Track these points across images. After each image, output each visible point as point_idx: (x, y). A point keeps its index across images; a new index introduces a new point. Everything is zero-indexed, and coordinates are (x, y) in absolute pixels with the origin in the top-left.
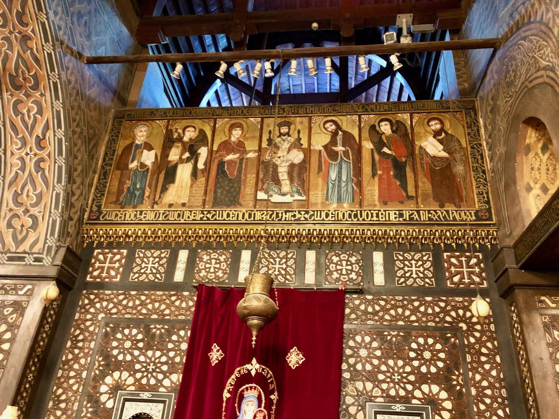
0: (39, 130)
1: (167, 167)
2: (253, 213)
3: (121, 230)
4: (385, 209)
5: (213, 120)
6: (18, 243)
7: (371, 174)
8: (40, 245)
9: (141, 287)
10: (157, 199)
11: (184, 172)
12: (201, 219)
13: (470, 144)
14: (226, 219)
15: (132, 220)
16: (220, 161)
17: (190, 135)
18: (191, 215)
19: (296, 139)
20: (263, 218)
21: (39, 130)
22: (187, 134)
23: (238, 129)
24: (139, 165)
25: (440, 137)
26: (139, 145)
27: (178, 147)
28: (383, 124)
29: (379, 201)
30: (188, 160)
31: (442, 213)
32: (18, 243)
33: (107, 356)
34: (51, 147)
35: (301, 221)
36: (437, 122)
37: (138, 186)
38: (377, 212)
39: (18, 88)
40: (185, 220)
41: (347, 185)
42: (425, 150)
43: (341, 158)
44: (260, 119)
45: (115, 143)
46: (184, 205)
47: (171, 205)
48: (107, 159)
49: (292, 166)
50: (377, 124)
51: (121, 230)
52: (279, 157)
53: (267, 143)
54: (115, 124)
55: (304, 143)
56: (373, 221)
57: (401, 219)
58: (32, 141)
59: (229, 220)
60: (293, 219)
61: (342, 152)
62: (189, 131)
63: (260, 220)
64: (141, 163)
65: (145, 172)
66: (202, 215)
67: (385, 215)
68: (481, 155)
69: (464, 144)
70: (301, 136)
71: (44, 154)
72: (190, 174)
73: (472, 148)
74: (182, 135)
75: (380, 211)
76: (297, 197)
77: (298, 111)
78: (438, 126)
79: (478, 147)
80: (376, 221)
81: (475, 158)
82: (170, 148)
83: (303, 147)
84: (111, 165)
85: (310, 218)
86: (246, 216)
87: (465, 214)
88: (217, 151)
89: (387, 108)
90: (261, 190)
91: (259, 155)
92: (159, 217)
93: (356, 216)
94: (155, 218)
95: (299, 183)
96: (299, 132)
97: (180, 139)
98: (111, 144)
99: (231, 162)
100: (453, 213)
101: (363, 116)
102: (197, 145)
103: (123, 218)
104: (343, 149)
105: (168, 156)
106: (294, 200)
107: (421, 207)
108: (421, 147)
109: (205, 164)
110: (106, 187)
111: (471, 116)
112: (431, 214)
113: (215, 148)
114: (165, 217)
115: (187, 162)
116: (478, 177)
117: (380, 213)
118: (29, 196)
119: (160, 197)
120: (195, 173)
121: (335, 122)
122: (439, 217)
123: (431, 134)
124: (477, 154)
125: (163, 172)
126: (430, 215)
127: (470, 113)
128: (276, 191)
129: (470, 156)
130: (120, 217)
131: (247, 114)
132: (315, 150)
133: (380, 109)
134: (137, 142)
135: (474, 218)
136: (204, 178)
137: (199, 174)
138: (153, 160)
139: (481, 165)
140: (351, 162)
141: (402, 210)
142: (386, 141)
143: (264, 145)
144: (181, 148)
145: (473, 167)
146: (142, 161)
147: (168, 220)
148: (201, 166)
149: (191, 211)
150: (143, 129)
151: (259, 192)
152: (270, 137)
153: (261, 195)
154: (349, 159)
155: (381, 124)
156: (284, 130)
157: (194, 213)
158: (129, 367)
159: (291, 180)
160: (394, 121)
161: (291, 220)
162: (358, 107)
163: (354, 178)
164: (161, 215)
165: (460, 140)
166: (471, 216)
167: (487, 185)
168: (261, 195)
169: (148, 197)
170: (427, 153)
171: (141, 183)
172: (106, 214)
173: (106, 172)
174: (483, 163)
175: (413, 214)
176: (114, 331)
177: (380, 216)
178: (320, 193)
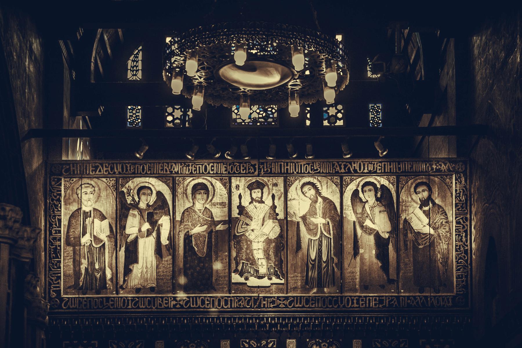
1: (127, 242)
2: (229, 298)
4: (366, 295)
5: (171, 179)
7: (353, 253)
10: (121, 283)
12: (175, 306)
13: (456, 218)
14: (201, 306)
15: (98, 308)
16: (185, 235)
18: (162, 301)
19: (271, 207)
20: (240, 305)
22: (143, 198)
23: (202, 191)
24: (92, 239)
25: (426, 208)
26: (88, 213)
27: (134, 216)
28: (367, 188)
29: (360, 286)
30: (149, 233)
31: (421, 299)
35: (280, 308)
36: (425, 188)
37: (97, 267)
38: (357, 298)
40: (156, 308)
41: (327, 265)
42: (409, 224)
43: (322, 233)
44: (227, 178)
45: (58, 211)
46: (152, 289)
47: (138, 290)
48: (53, 232)
49: (268, 241)
50: (360, 189)
52: (253, 230)
53: (238, 211)
54: (53, 183)
55: (280, 210)
56: (354, 307)
57: (381, 306)
59: (205, 308)
60: (272, 306)
61: (322, 225)
62: (144, 194)
63: (237, 308)
64: (94, 236)
65: (102, 249)
66: (174, 302)
67: (366, 302)
68: (466, 232)
69: (450, 219)
70: (276, 204)
72: (153, 251)
73: (457, 223)
74: (137, 199)
75: (361, 297)
76: (275, 280)
77: (271, 169)
78: (426, 194)
79: (464, 222)
80: (356, 307)
81: (459, 235)
82: (126, 217)
83: (278, 217)
84: (60, 240)
85: (290, 304)
86: (223, 303)
87: (443, 299)
88: (181, 222)
89: (372, 169)
90: (236, 271)
91: (229, 229)
92: (128, 305)
93: (336, 302)
94: (124, 305)
95: (277, 263)
96: (273, 197)
97: (135, 206)
98: (53, 211)
99: (198, 235)
100: (431, 299)
101: (344, 178)
102: (157, 213)
103: (88, 306)
104: (323, 221)
105: (124, 228)
106: (272, 284)
107: (401, 292)
108: (406, 221)
109: (169, 238)
110: (60, 268)
111: (461, 182)
112: (411, 300)
113: (178, 218)
114: (135, 305)
115: (147, 236)
116: (461, 258)
117: (361, 299)
119: (125, 281)
120: (159, 250)
121: (313, 185)
122: (417, 303)
123: (417, 203)
124: (462, 230)
125: (123, 249)
126: (409, 301)
127: (460, 177)
128: (252, 272)
129: (454, 233)
130: (85, 305)
131: (211, 172)
132: (292, 221)
133: (364, 169)
134: (84, 208)
135: (450, 304)
136: (170, 257)
137: (164, 250)
138: (108, 233)
139: (464, 244)
140: (332, 237)
141: (383, 296)
142: (369, 212)
143: (235, 213)
144: (138, 217)
145: (456, 246)
146: (95, 234)
147: (138, 308)
148: (164, 241)
149: (162, 298)
150: (89, 190)
151: (233, 274)
152: (240, 203)
153: (236, 278)
154: (330, 234)
155: (365, 189)
156: (256, 194)
157: (166, 300)
159: (268, 258)
160: (379, 186)
161: (271, 308)
162: (340, 165)
163: (335, 258)
164: (130, 301)
165: (447, 212)
166: (449, 302)
167: (468, 267)
168: (236, 278)
169: (111, 280)
170: (411, 228)
171: (99, 262)
172: (68, 301)
173: (56, 248)
174: (467, 241)
175: (392, 300)
177: (361, 303)
178: (299, 275)
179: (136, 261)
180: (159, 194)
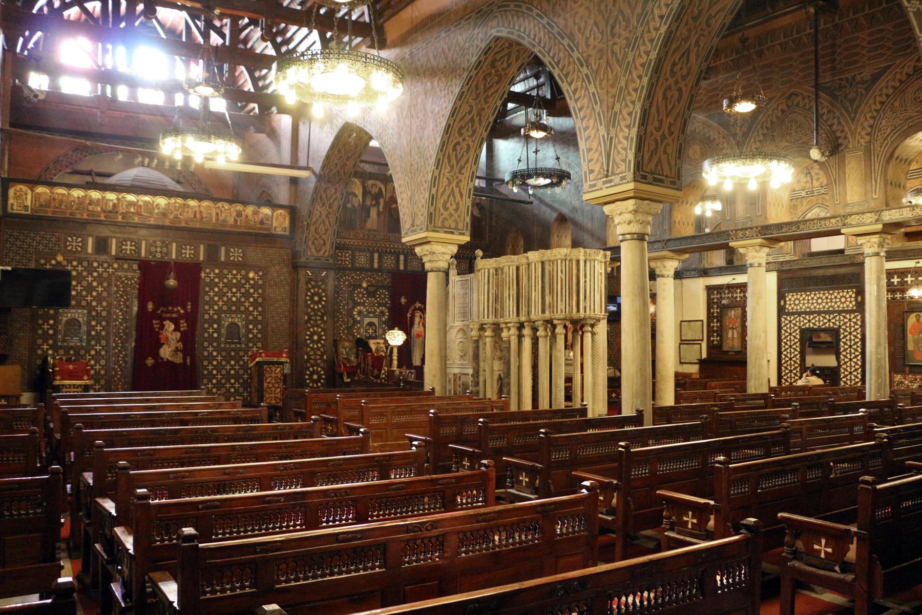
0: (332, 201)
3: (347, 241)
6: (318, 251)
8: (327, 254)
9: (361, 270)
11: (373, 213)
17: (375, 190)
21: (332, 201)
30: (375, 205)
32: (318, 251)
33: (354, 300)
34: (335, 208)
39: (329, 182)
51: (347, 241)
58: (327, 204)
71: (331, 210)
118: (322, 228)
120: (379, 214)
148: (381, 210)
158: (363, 304)
176: (354, 290)
179: (369, 217)
180: (380, 189)
